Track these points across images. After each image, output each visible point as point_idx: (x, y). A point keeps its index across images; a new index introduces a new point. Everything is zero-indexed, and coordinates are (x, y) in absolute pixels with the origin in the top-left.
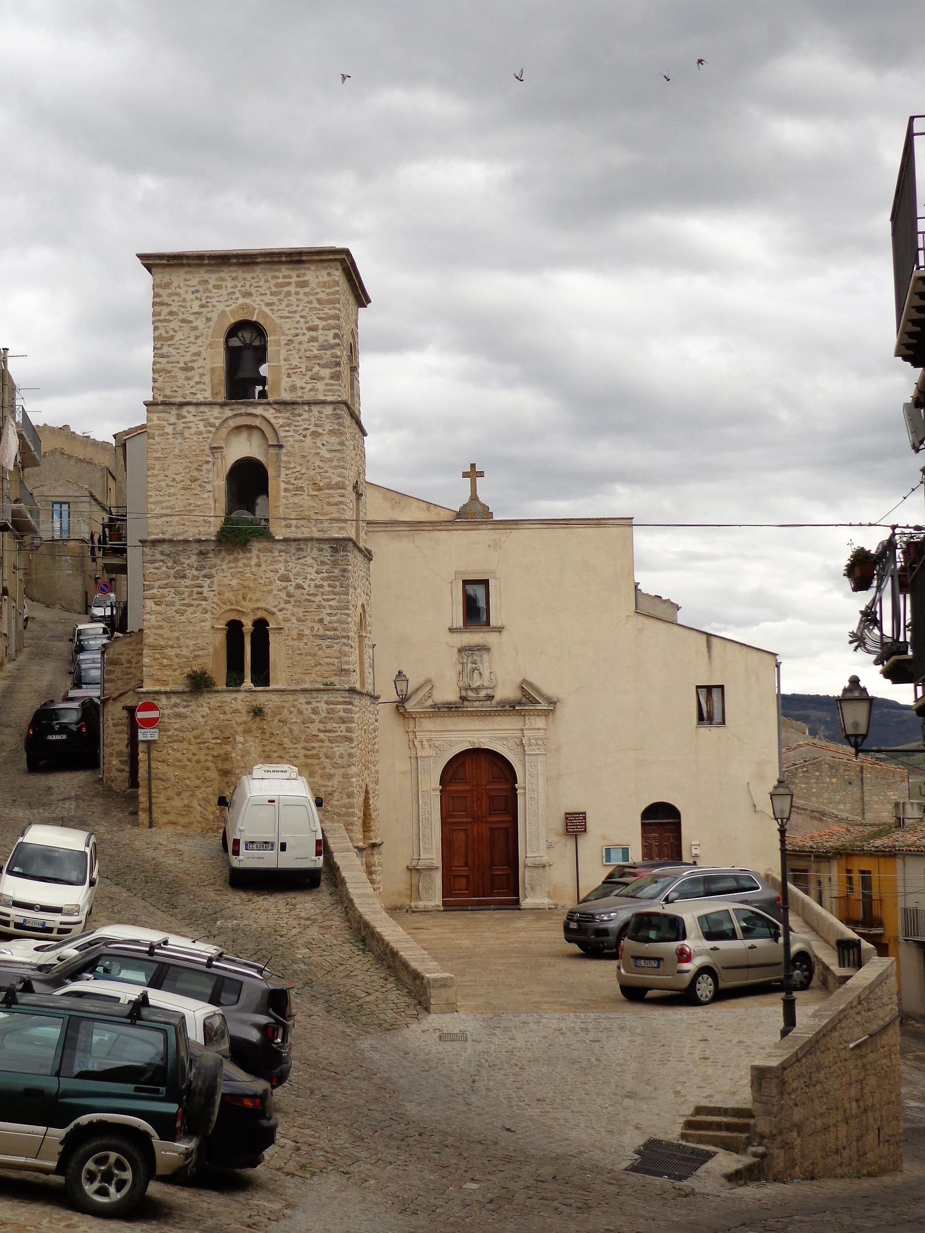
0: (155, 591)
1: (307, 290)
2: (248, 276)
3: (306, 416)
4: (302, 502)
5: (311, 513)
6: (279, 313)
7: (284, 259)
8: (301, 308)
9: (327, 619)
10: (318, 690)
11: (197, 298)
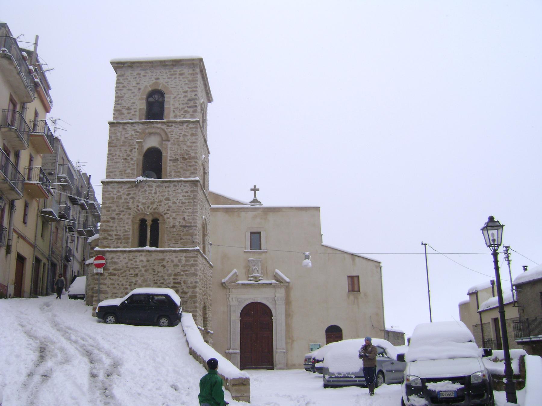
1: (184, 76)
9: (187, 218)
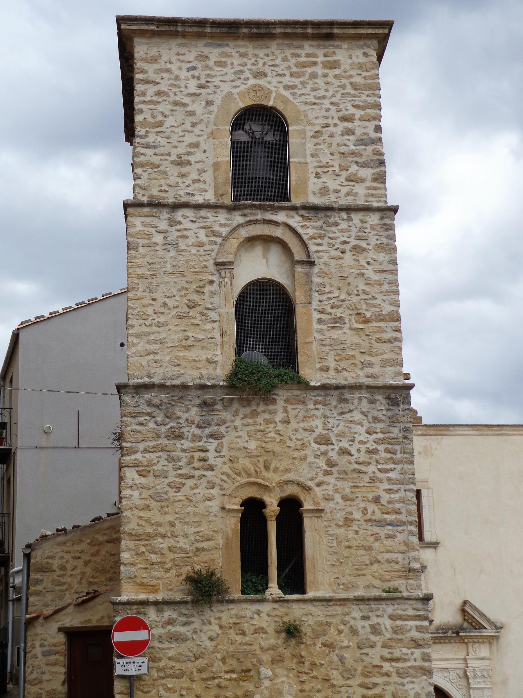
0: (138, 456)
1: (337, 71)
2: (261, 53)
3: (344, 225)
4: (342, 338)
5: (356, 353)
6: (303, 98)
7: (310, 31)
8: (329, 94)
9: (385, 498)
10: (378, 599)
11: (193, 77)
